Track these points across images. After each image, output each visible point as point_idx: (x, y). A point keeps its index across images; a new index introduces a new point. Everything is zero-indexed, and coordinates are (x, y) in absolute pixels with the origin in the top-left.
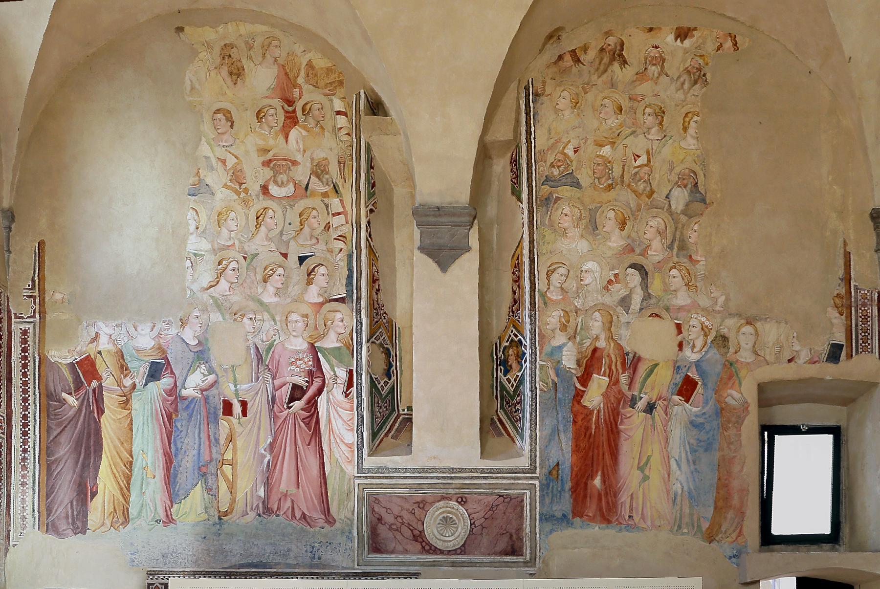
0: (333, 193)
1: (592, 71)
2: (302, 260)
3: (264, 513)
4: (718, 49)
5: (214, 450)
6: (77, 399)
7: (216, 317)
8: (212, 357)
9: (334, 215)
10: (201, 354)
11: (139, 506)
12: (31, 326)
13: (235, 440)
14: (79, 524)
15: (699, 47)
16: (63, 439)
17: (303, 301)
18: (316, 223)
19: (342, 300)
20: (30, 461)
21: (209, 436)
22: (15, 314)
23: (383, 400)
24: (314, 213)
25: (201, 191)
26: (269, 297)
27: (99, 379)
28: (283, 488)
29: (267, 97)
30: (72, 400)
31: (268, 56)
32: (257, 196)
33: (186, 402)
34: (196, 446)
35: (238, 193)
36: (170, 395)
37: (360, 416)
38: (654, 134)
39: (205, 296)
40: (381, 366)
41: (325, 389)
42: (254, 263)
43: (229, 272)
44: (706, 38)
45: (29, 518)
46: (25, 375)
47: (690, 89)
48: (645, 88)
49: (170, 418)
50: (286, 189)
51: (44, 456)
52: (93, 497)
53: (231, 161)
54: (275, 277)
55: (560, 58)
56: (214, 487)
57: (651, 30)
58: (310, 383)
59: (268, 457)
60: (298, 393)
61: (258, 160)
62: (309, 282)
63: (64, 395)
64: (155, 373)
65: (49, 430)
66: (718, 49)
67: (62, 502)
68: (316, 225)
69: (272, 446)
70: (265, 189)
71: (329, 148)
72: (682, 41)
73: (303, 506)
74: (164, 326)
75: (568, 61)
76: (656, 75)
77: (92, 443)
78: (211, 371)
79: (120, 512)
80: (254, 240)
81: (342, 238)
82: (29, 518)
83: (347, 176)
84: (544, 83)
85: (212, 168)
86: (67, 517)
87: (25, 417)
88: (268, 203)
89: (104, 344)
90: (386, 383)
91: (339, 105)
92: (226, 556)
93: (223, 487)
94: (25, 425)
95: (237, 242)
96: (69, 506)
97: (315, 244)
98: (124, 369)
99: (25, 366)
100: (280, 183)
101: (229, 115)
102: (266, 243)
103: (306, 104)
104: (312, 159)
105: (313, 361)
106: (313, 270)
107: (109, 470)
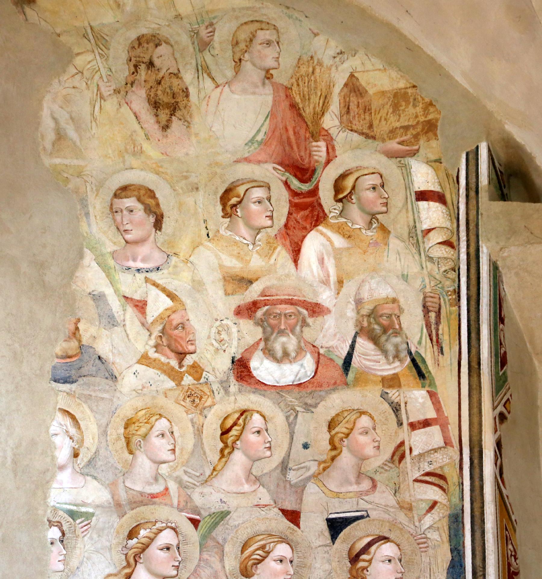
0: (410, 377)
2: (336, 526)
9: (413, 426)
18: (371, 443)
24: (364, 421)
25: (84, 371)
29: (247, 160)
31: (247, 66)
32: (224, 385)
35: (176, 376)
42: (219, 533)
43: (154, 551)
50: (295, 367)
53: (158, 304)
54: (270, 564)
61: (224, 304)
68: (369, 451)
70: (241, 368)
71: (400, 277)
80: (216, 482)
81: (436, 478)
83: (445, 339)
85: (111, 321)
88: (250, 400)
91: (423, 177)
95: (173, 487)
97: (367, 493)
100: (279, 354)
101: (151, 202)
102: (247, 488)
103: (343, 176)
104: (359, 302)
106: (366, 549)
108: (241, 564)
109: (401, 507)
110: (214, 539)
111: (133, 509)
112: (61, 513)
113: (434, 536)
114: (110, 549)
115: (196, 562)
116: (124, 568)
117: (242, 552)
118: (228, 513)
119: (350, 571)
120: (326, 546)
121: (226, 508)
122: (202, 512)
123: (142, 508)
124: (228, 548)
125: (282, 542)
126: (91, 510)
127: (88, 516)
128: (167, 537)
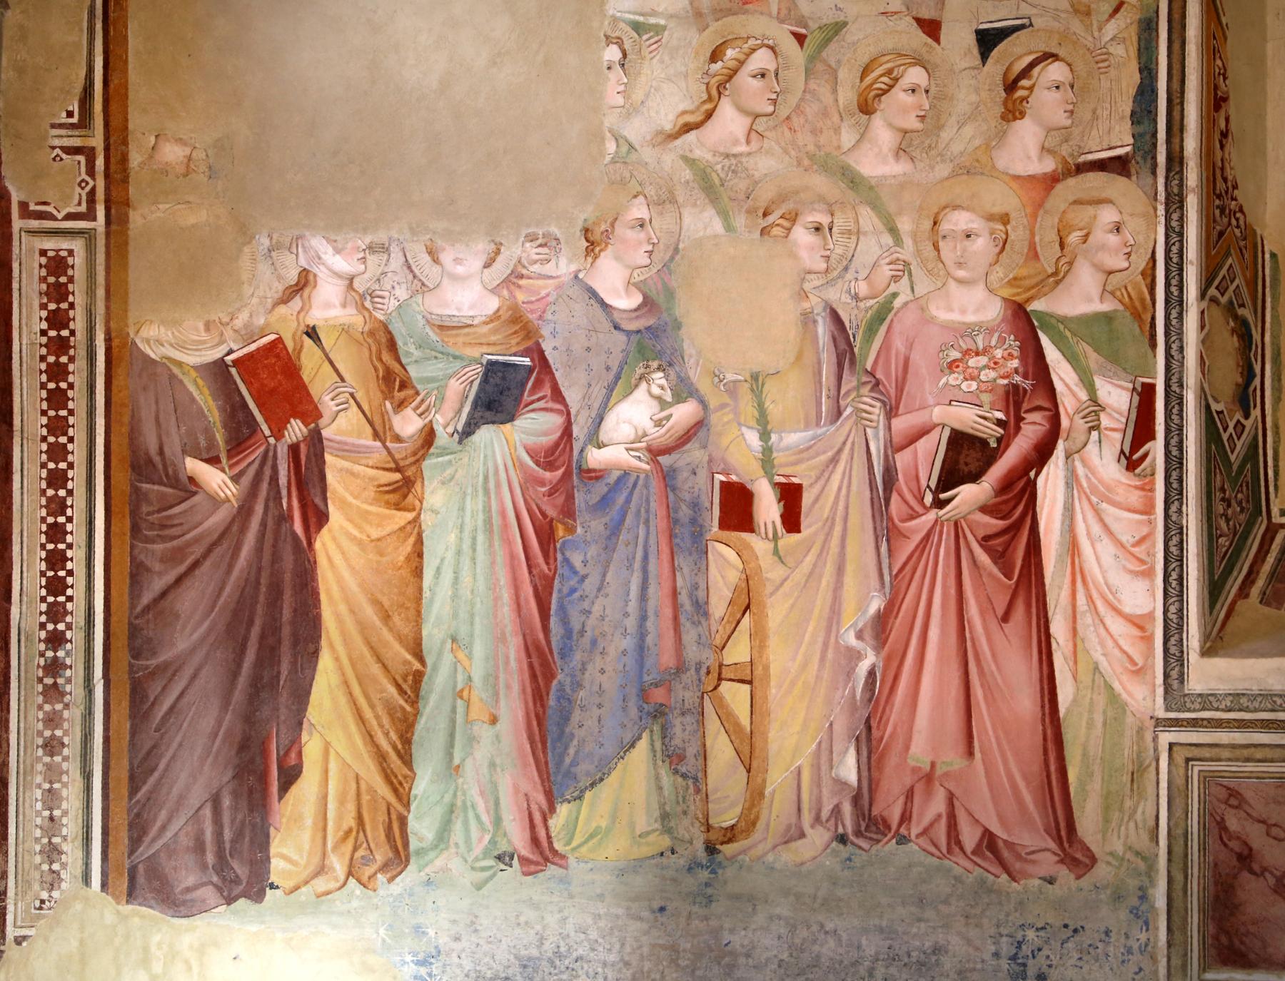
2: (988, 40)
3: (858, 833)
5: (690, 636)
6: (236, 479)
7: (701, 222)
8: (688, 349)
10: (651, 341)
11: (439, 811)
12: (78, 245)
13: (762, 606)
14: (241, 869)
16: (190, 600)
17: (991, 172)
19: (1119, 166)
20: (75, 673)
21: (675, 593)
22: (23, 206)
23: (1234, 481)
26: (877, 160)
27: (310, 413)
28: (919, 753)
30: (215, 479)
33: (600, 489)
34: (631, 623)
36: (549, 466)
37: (1174, 531)
39: (669, 159)
40: (1229, 375)
41: (1060, 446)
42: (831, 53)
43: (745, 79)
45: (72, 852)
46: (57, 399)
49: (546, 536)
51: (122, 656)
52: (285, 787)
54: (899, 96)
56: (691, 751)
58: (1010, 427)
59: (869, 659)
60: (970, 459)
62: (1013, 111)
63: (194, 466)
64: (498, 396)
65: (138, 573)
67: (181, 798)
69: (882, 624)
73: (984, 811)
74: (532, 251)
77: (287, 614)
78: (684, 390)
79: (376, 833)
82: (72, 852)
86: (199, 847)
87: (56, 533)
89: (328, 305)
90: (1240, 427)
92: (732, 967)
93: (722, 751)
94: (56, 560)
96: (207, 812)
98: (395, 384)
99: (57, 372)
105: (1023, 358)
106: (1026, 73)
107: (343, 700)
108: (860, 95)
109: (1076, 11)
110: (824, 61)
111: (717, 20)
112: (622, 25)
113: (1118, 50)
114: (686, 76)
115: (799, 94)
116: (704, 102)
117: (862, 80)
118: (845, 24)
119: (1005, 103)
120: (974, 68)
121: (842, 18)
122: (811, 23)
123: (730, 19)
124: (842, 74)
125: (914, 64)
126: (662, 22)
127: (659, 30)
128: (762, 59)
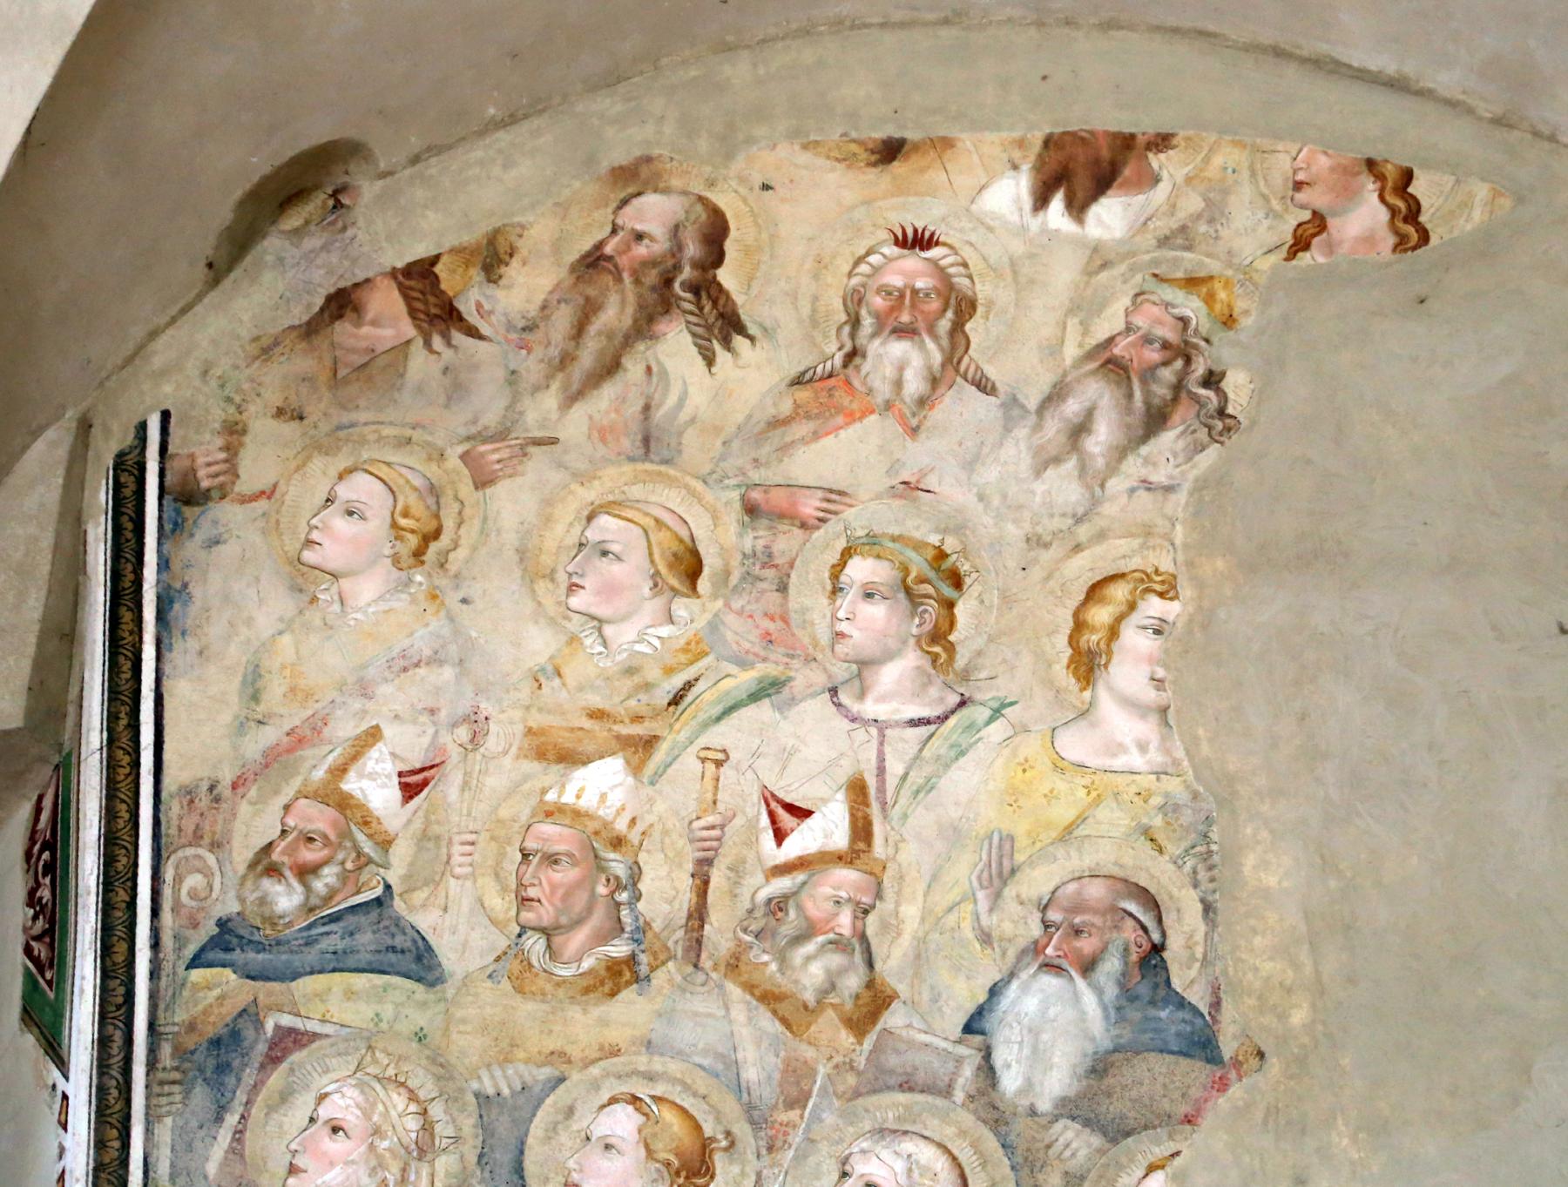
1: (531, 366)
4: (1300, 244)
15: (1181, 237)
38: (897, 688)
44: (1225, 194)
47: (1121, 453)
48: (846, 455)
55: (343, 303)
57: (890, 151)
66: (1300, 244)
72: (1077, 208)
75: (388, 318)
76: (914, 385)
84: (234, 432)
